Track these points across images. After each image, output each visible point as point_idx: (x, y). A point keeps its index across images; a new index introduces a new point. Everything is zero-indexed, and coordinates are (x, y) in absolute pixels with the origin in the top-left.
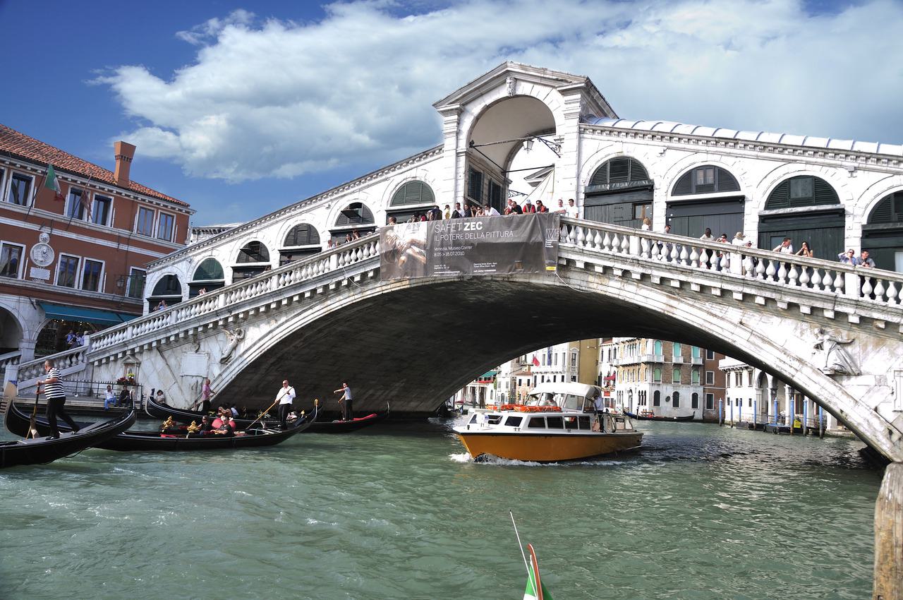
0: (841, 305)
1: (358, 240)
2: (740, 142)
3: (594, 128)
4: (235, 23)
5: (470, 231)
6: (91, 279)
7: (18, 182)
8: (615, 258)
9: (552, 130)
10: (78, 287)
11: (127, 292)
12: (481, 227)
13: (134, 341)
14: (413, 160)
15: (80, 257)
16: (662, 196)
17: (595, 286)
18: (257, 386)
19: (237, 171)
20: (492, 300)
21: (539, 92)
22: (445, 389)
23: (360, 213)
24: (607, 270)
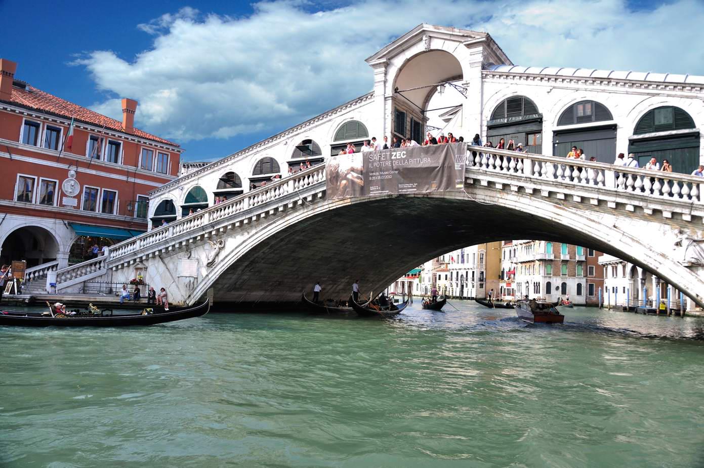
0: (697, 210)
1: (311, 168)
2: (612, 80)
3: (494, 73)
4: (183, 17)
5: (397, 159)
6: (108, 204)
8: (512, 177)
9: (460, 77)
10: (98, 212)
11: (136, 213)
12: (405, 156)
13: (142, 251)
14: (351, 104)
15: (99, 188)
16: (550, 126)
17: (496, 199)
18: (235, 284)
19: (185, 132)
20: (415, 213)
21: (449, 47)
22: (381, 283)
23: (311, 148)
24: (505, 187)
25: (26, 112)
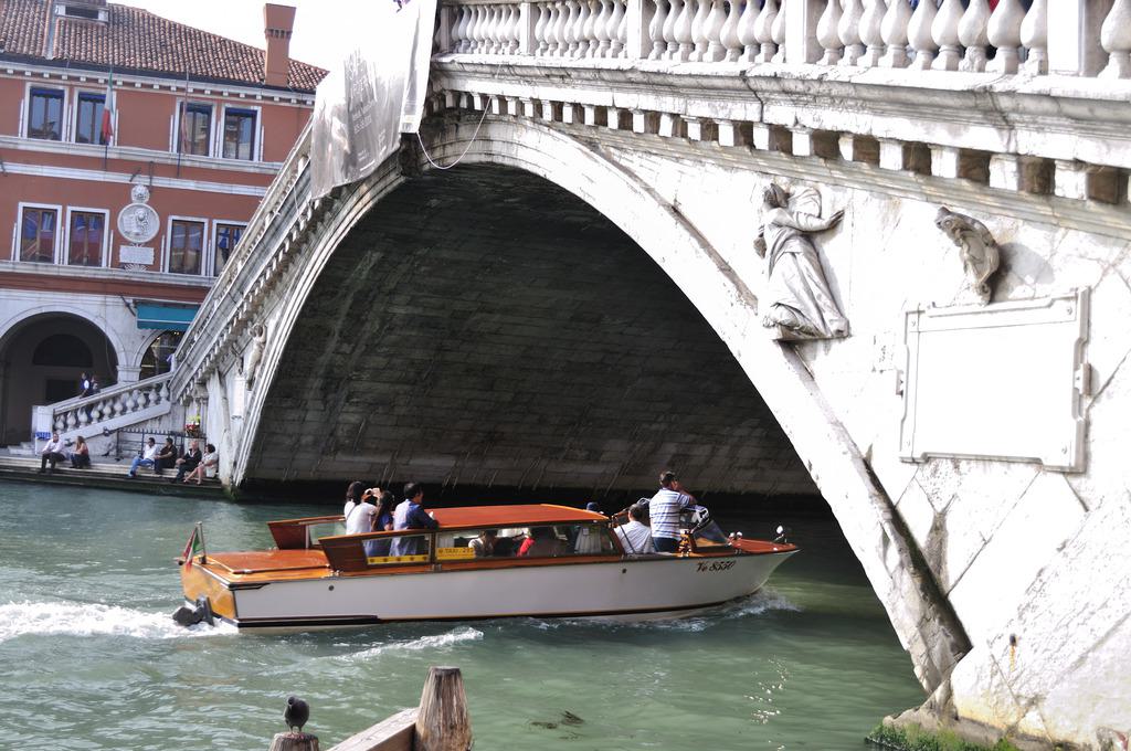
7: (47, 101)
15: (205, 221)
25: (28, 70)
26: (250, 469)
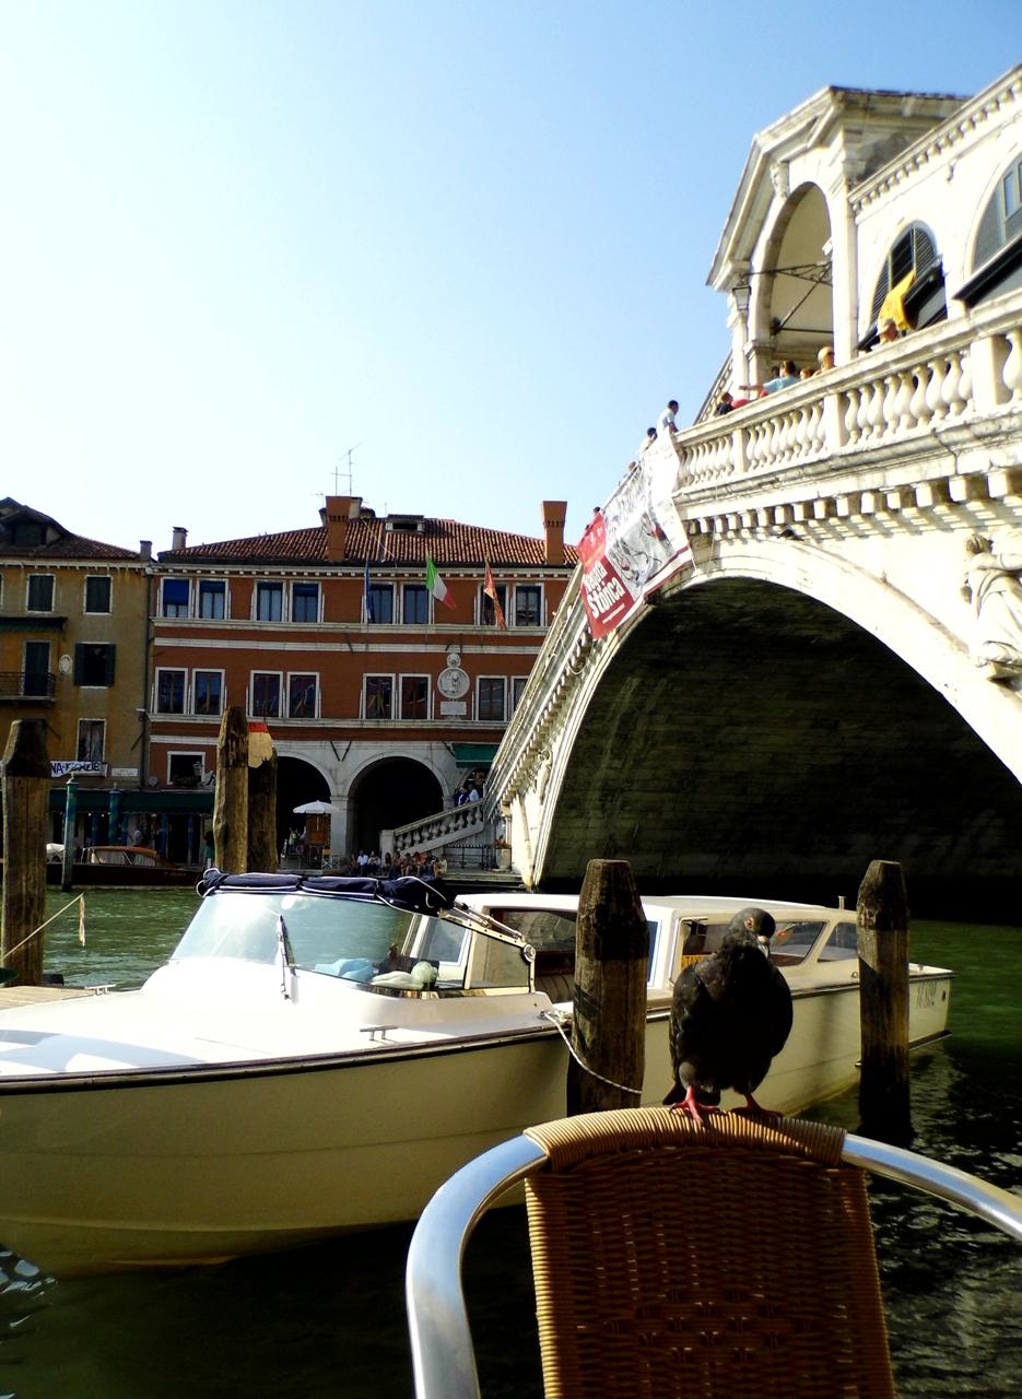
15: (505, 677)
26: (546, 869)
